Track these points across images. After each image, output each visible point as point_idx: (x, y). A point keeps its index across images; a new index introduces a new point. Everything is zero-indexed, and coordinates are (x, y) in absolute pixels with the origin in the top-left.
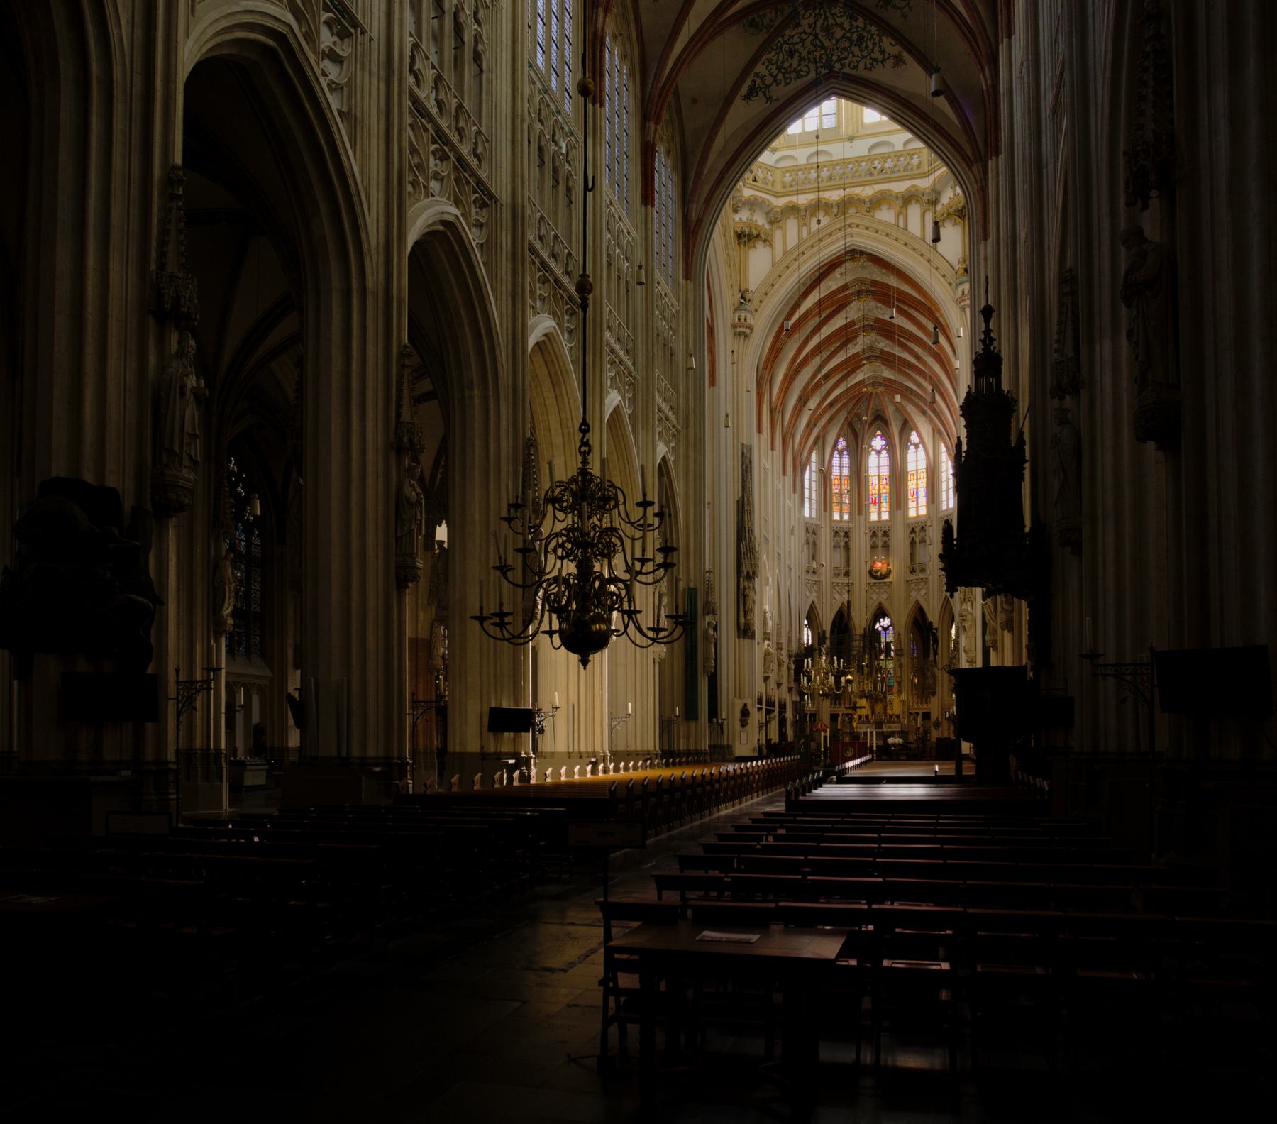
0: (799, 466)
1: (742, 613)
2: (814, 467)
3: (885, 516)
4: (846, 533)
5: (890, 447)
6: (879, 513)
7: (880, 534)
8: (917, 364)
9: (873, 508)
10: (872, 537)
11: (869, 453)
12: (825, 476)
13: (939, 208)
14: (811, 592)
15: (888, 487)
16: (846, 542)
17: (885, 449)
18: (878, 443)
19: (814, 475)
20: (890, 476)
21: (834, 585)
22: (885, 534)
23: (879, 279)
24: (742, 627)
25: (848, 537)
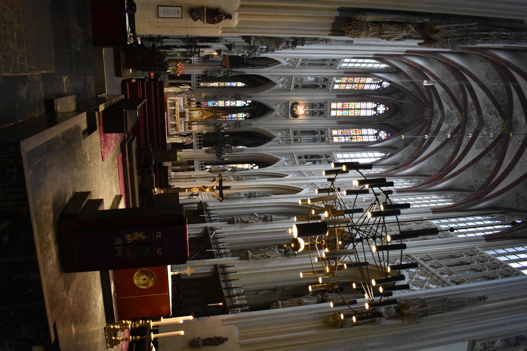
0: (379, 58)
1: (381, 18)
2: (376, 66)
3: (333, 113)
4: (326, 86)
6: (336, 109)
7: (322, 110)
8: (460, 152)
9: (339, 105)
10: (320, 104)
11: (375, 103)
12: (366, 73)
14: (288, 62)
15: (353, 115)
16: (319, 86)
17: (377, 113)
18: (381, 109)
19: (370, 66)
20: (360, 116)
21: (290, 78)
22: (321, 113)
24: (358, 17)
25: (323, 88)
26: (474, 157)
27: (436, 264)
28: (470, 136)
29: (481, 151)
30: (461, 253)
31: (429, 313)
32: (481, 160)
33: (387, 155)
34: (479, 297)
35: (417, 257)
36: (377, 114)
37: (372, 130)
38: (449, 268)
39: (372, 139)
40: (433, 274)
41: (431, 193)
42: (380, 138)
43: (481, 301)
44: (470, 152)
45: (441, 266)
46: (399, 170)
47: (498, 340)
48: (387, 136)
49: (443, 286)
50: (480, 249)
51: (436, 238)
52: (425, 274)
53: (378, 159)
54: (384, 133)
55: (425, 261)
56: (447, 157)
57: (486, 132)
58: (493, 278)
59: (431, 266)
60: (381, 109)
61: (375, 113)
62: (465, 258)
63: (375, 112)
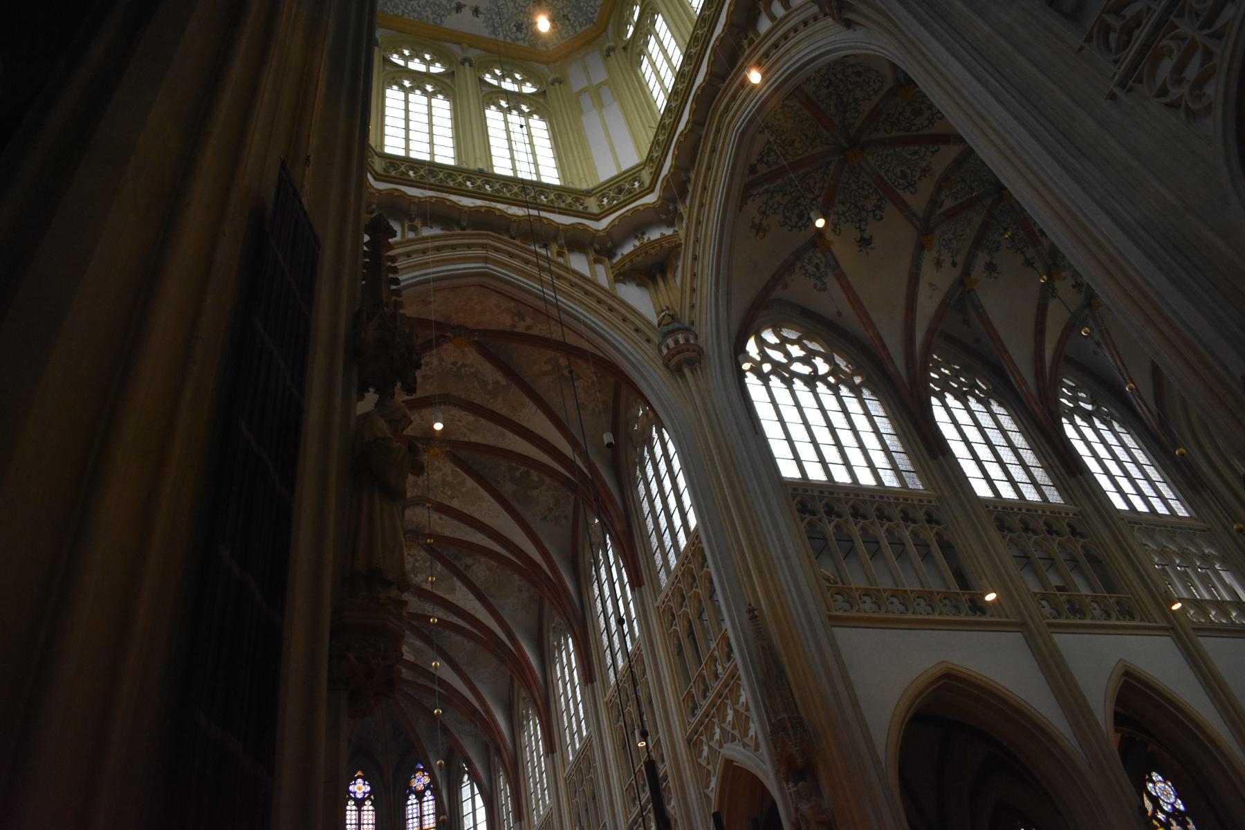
5: (377, 796)
8: (461, 623)
13: (615, 261)
17: (369, 798)
18: (360, 788)
23: (478, 401)
26: (471, 596)
27: (699, 686)
28: (434, 620)
29: (458, 584)
30: (670, 634)
31: (796, 715)
32: (478, 584)
33: (466, 769)
34: (750, 619)
35: (689, 723)
36: (372, 797)
37: (410, 807)
38: (704, 663)
39: (429, 806)
40: (719, 695)
41: (549, 679)
42: (427, 787)
43: (756, 617)
44: (461, 604)
45: (701, 676)
46: (501, 746)
47: (821, 571)
48: (423, 771)
49: (739, 678)
50: (661, 598)
51: (647, 679)
52: (721, 710)
53: (476, 791)
54: (415, 778)
55: (695, 708)
56: (469, 645)
57: (419, 575)
58: (711, 582)
59: (705, 697)
60: (360, 789)
61: (368, 803)
62: (680, 627)
63: (366, 803)
